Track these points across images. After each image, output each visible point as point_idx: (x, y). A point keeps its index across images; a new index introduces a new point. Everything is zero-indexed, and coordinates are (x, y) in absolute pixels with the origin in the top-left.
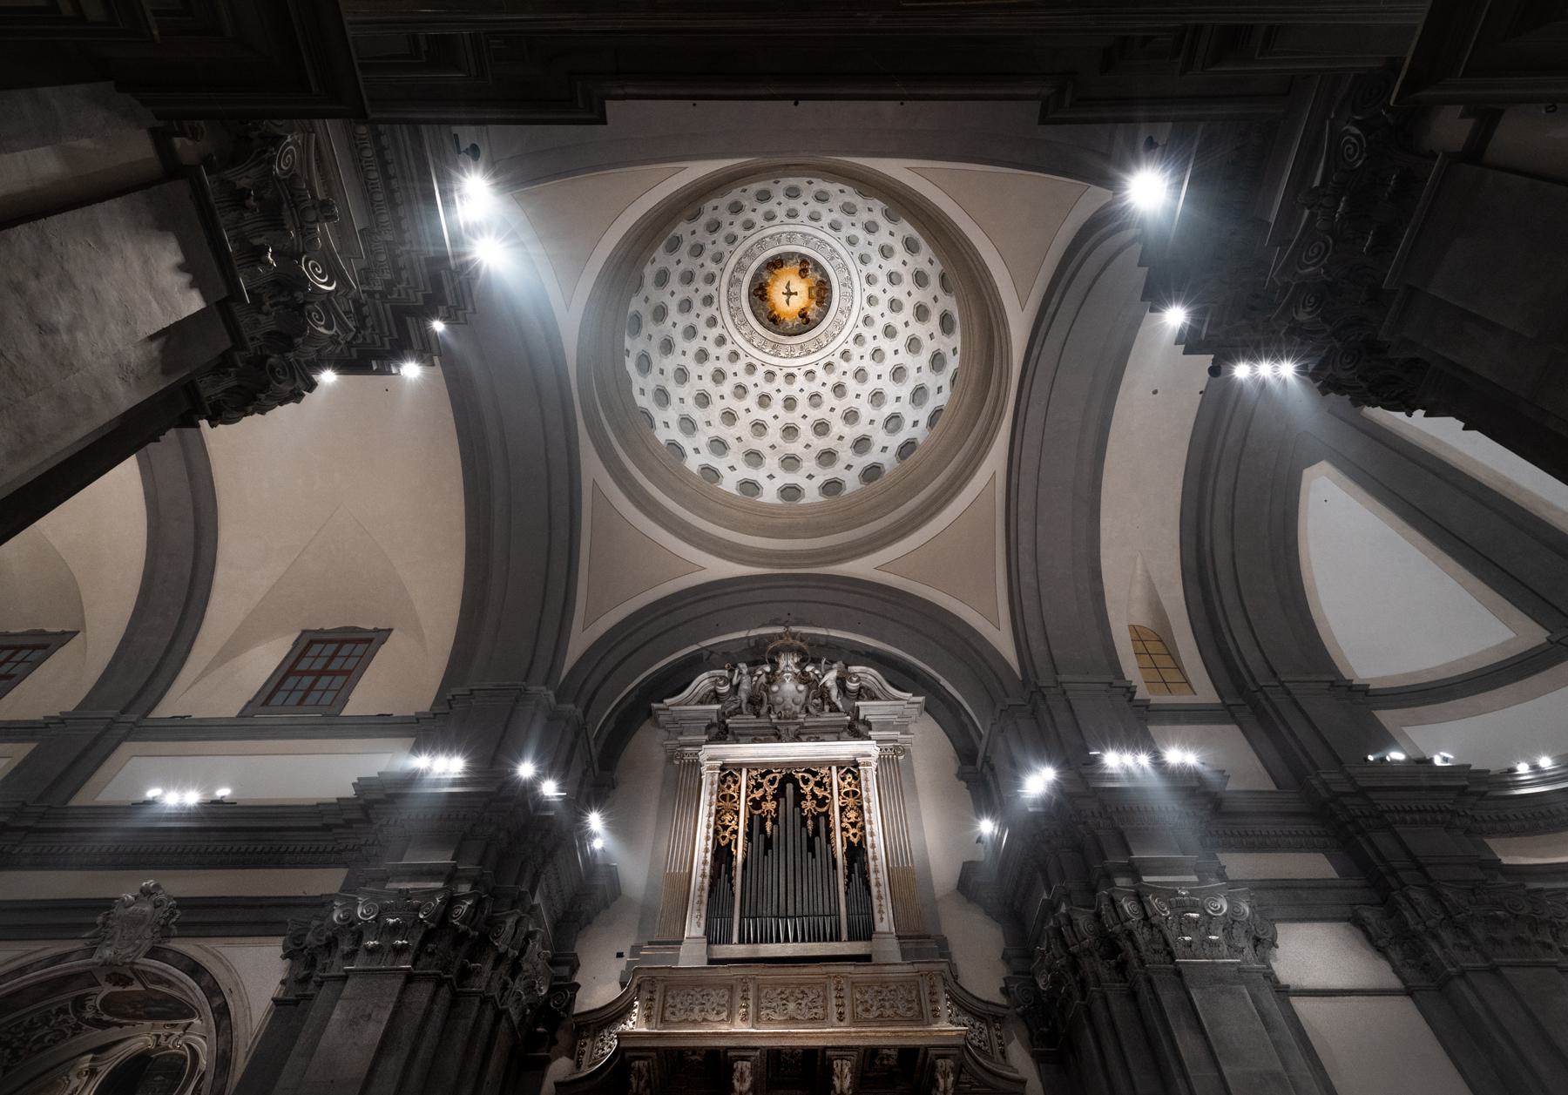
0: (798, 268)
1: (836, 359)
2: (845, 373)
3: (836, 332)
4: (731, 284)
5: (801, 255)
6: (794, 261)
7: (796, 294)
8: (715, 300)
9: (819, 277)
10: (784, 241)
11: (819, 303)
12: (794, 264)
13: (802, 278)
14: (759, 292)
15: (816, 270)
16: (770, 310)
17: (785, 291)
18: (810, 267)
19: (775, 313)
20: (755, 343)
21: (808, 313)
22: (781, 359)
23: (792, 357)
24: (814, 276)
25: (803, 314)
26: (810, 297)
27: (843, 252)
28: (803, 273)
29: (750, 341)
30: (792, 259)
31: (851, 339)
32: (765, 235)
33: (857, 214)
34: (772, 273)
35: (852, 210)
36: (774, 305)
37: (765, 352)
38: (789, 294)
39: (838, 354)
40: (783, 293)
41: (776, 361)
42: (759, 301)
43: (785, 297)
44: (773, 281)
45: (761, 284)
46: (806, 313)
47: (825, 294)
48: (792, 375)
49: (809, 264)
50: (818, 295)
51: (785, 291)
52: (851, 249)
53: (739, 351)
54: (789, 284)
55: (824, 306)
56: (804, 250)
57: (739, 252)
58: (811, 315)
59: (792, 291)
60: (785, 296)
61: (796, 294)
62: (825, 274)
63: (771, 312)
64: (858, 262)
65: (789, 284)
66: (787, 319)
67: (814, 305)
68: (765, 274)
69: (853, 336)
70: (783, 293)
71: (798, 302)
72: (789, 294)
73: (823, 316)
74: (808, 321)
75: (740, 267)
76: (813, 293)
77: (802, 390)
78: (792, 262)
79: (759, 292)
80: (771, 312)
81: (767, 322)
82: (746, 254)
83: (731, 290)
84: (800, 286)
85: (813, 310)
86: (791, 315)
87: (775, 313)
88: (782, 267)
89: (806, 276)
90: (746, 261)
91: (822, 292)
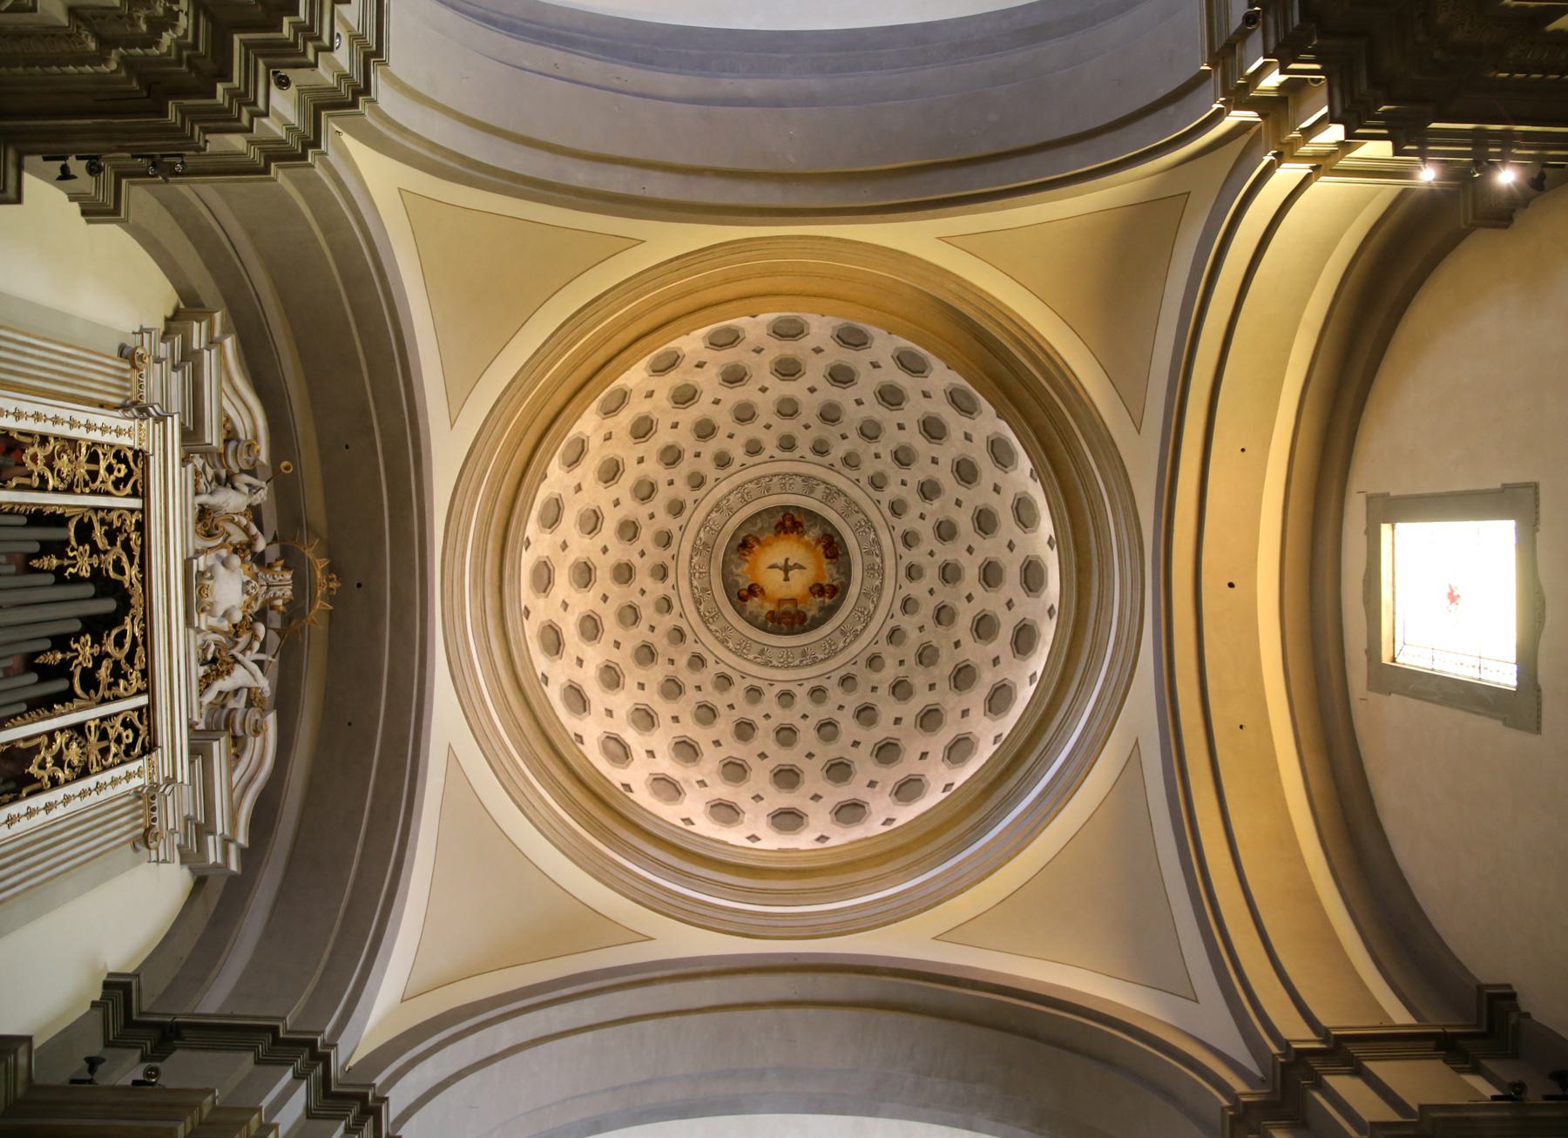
0: (826, 582)
1: (690, 646)
2: (672, 661)
3: (730, 645)
4: (807, 478)
5: (845, 587)
6: (836, 576)
7: (787, 579)
8: (787, 455)
9: (810, 614)
10: (868, 560)
11: (772, 616)
12: (831, 576)
13: (811, 589)
14: (790, 522)
15: (821, 609)
16: (761, 539)
17: (791, 563)
18: (827, 601)
19: (757, 547)
20: (714, 515)
21: (756, 599)
22: (688, 558)
23: (692, 575)
24: (812, 607)
25: (753, 590)
26: (780, 602)
27: (855, 648)
28: (818, 589)
29: (717, 507)
30: (838, 572)
31: (722, 668)
32: (879, 532)
33: (920, 668)
34: (818, 542)
35: (926, 661)
36: (769, 545)
37: (699, 530)
38: (786, 569)
39: (698, 649)
40: (787, 560)
41: (686, 548)
42: (775, 521)
43: (781, 562)
44: (807, 545)
45: (801, 525)
46: (756, 596)
47: (786, 624)
48: (664, 577)
49: (831, 597)
50: (785, 613)
51: (791, 563)
52: (862, 661)
53: (703, 490)
54: (801, 567)
55: (766, 623)
56: (854, 590)
57: (854, 492)
58: (753, 604)
59: (791, 574)
60: (783, 562)
61: (787, 579)
62: (817, 623)
63: (758, 541)
64: (843, 672)
65: (801, 567)
66: (746, 566)
67: (769, 607)
68: (813, 534)
69: (729, 672)
70: (787, 560)
71: (773, 582)
72: (786, 569)
73: (752, 621)
74: (743, 599)
75: (832, 493)
76: (787, 607)
77: (643, 592)
78: (834, 571)
79: (790, 522)
80: (758, 541)
81: (743, 534)
82: (851, 502)
83: (799, 479)
84: (798, 584)
85: (762, 606)
86: (753, 569)
87: (757, 547)
88: (827, 557)
89: (813, 594)
90: (840, 503)
91: (788, 620)
